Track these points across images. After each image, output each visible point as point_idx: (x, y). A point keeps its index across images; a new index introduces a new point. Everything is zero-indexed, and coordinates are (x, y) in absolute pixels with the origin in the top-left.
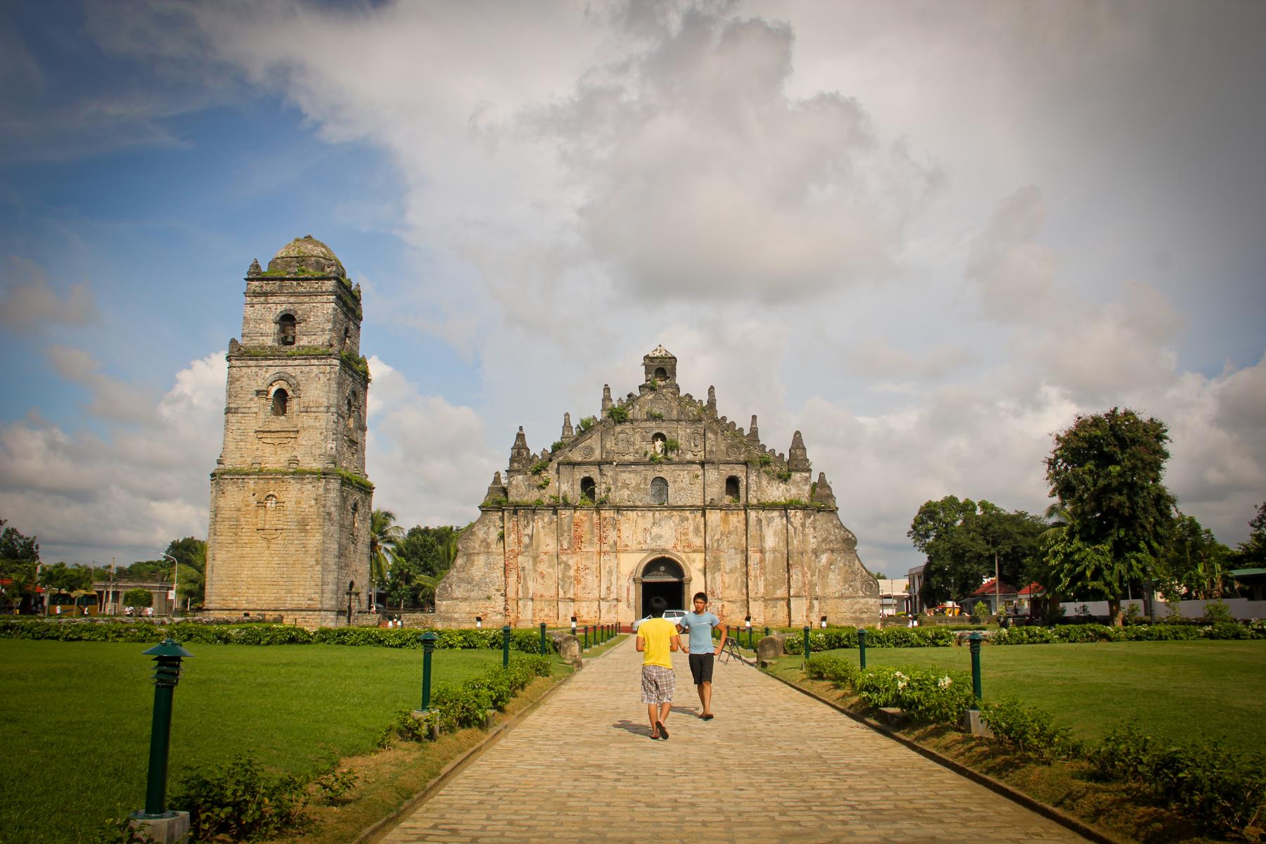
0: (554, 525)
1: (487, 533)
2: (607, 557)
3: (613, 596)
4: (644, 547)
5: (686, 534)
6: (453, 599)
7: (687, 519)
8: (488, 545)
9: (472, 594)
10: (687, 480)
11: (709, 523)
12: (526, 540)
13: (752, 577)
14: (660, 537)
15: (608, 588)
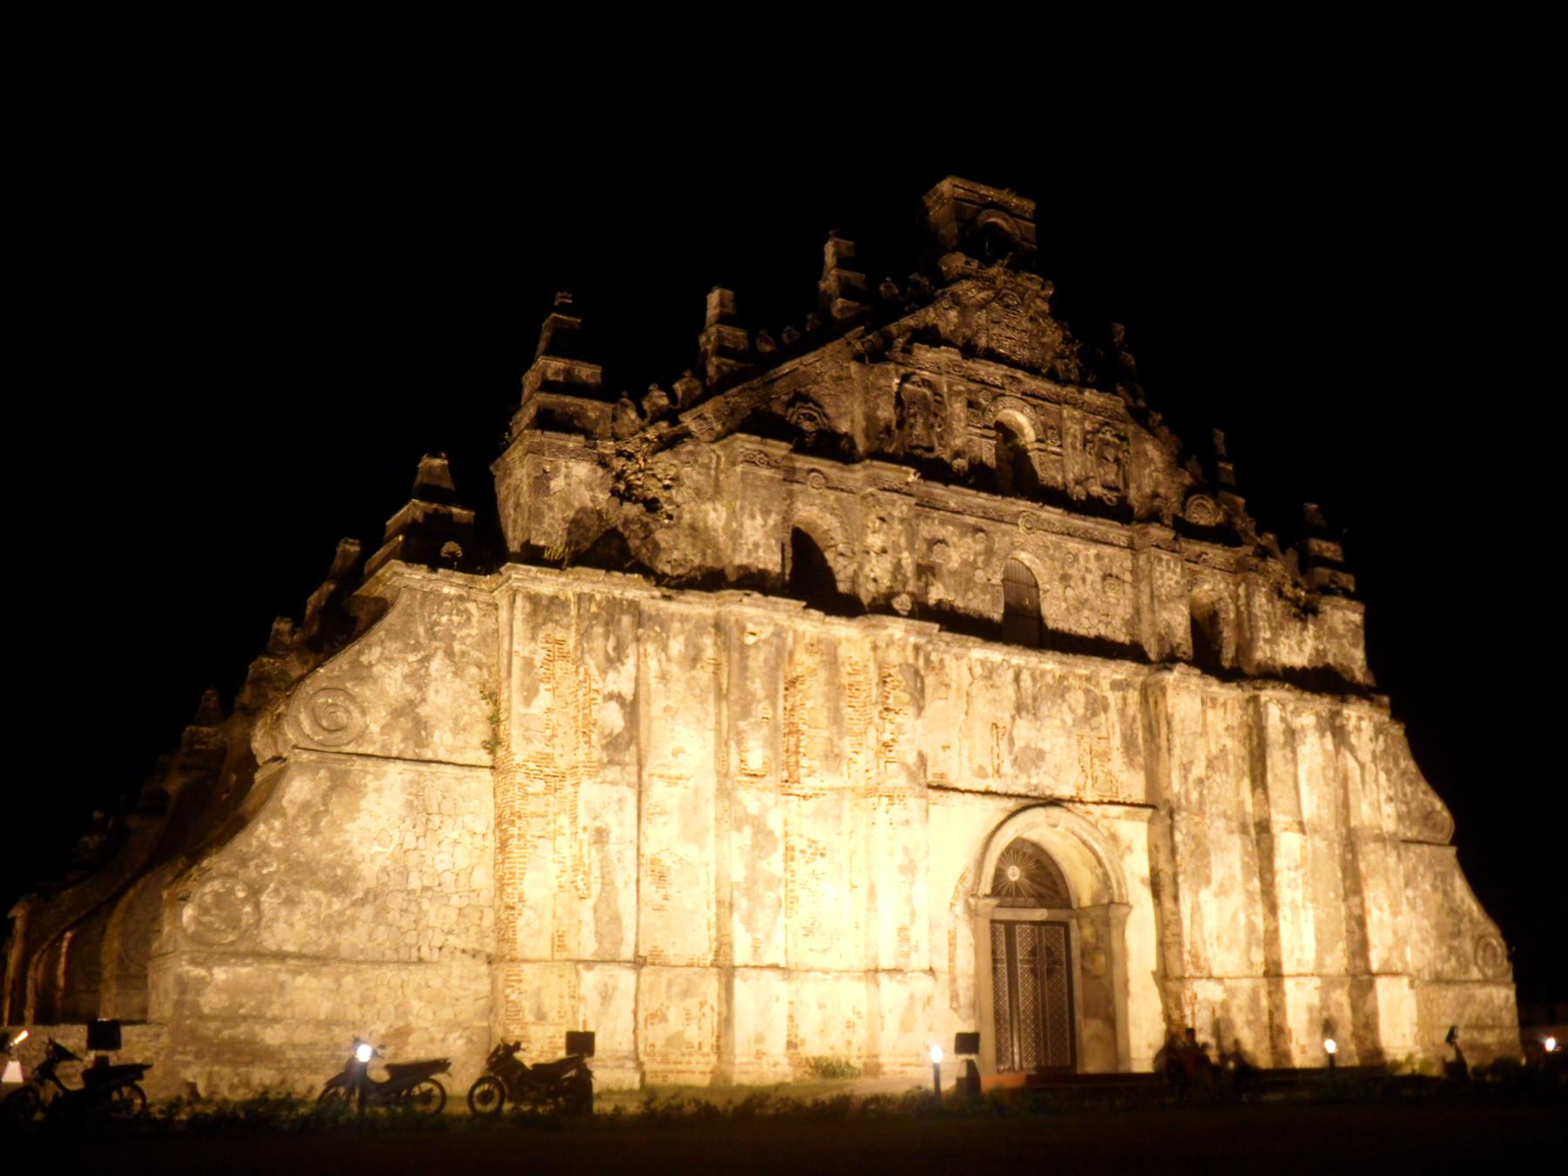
0: (704, 675)
1: (418, 679)
2: (897, 811)
3: (919, 961)
4: (994, 785)
5: (1105, 756)
6: (260, 955)
7: (1106, 709)
8: (420, 730)
9: (350, 940)
10: (1094, 577)
11: (1176, 724)
12: (613, 717)
13: (1284, 912)
14: (1040, 755)
15: (903, 934)
